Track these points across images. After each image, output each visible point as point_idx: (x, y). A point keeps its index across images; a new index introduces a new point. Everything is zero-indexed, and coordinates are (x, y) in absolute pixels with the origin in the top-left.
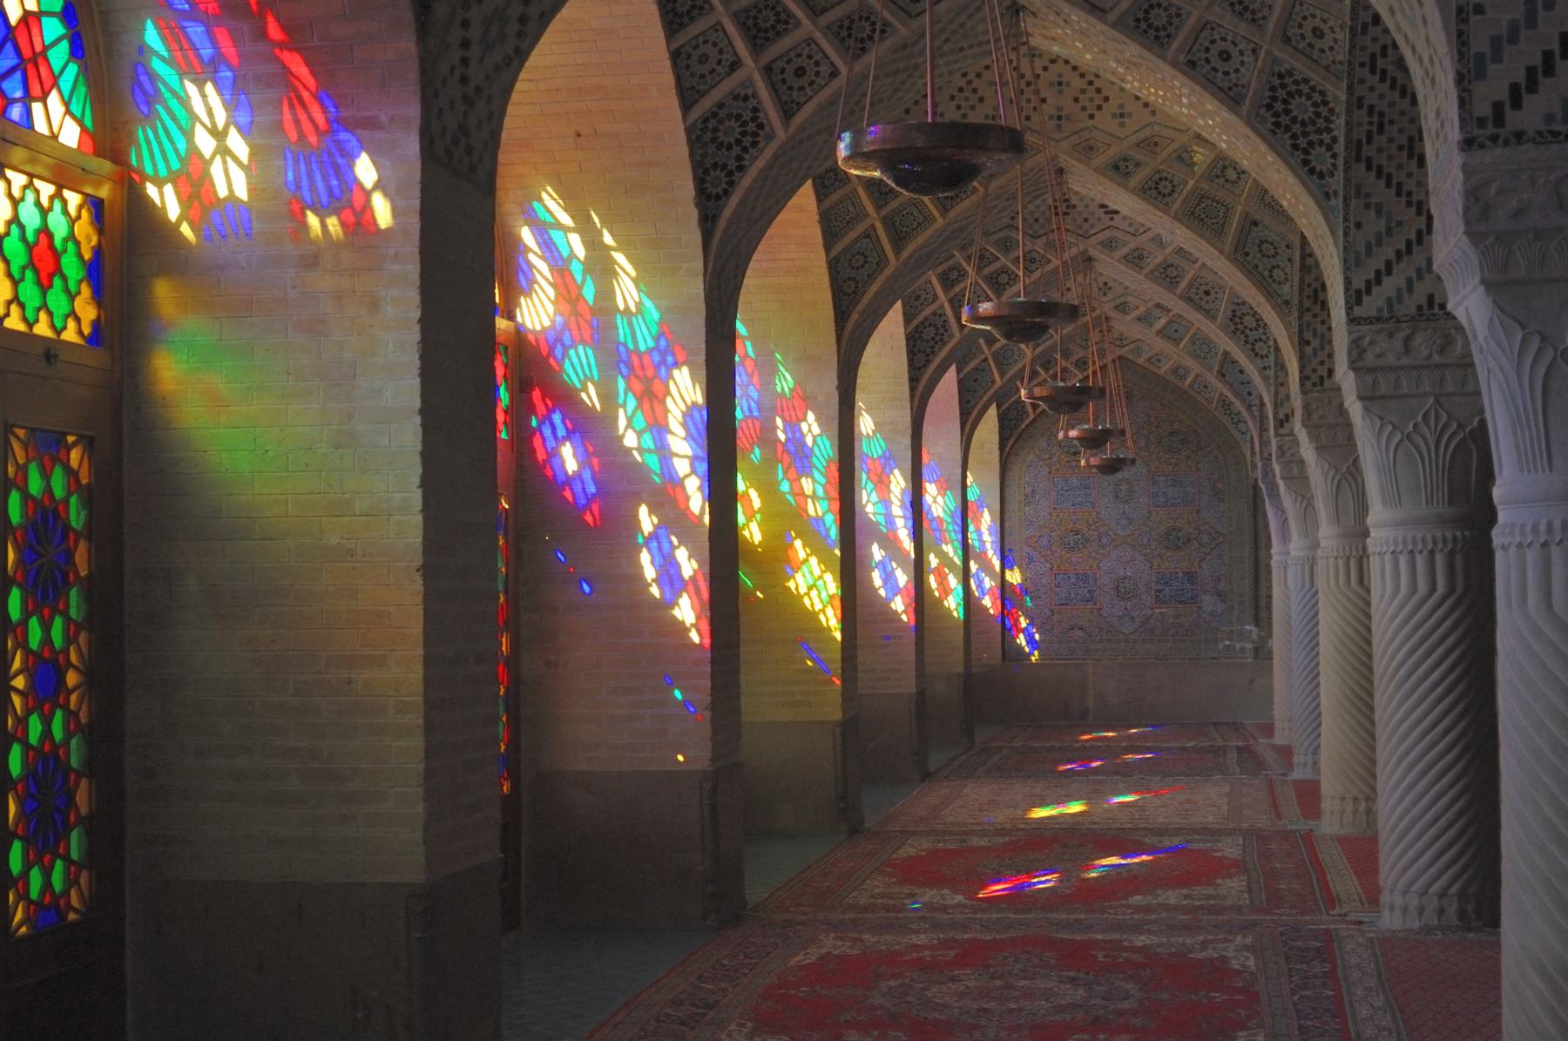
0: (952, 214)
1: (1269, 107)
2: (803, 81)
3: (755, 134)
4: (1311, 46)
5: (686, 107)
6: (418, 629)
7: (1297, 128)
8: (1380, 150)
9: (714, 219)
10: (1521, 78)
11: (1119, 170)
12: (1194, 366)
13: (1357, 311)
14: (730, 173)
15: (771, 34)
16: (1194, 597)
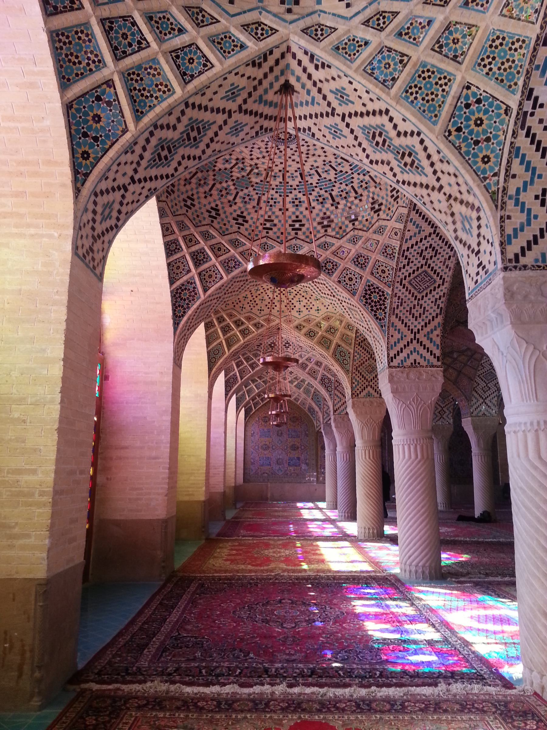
0: (246, 339)
1: (364, 297)
2: (211, 280)
3: (194, 296)
4: (380, 276)
5: (172, 283)
6: (53, 456)
7: (373, 304)
8: (401, 311)
9: (178, 324)
10: (525, 245)
11: (298, 328)
12: (304, 396)
13: (392, 364)
14: (185, 309)
15: (202, 262)
16: (299, 465)
